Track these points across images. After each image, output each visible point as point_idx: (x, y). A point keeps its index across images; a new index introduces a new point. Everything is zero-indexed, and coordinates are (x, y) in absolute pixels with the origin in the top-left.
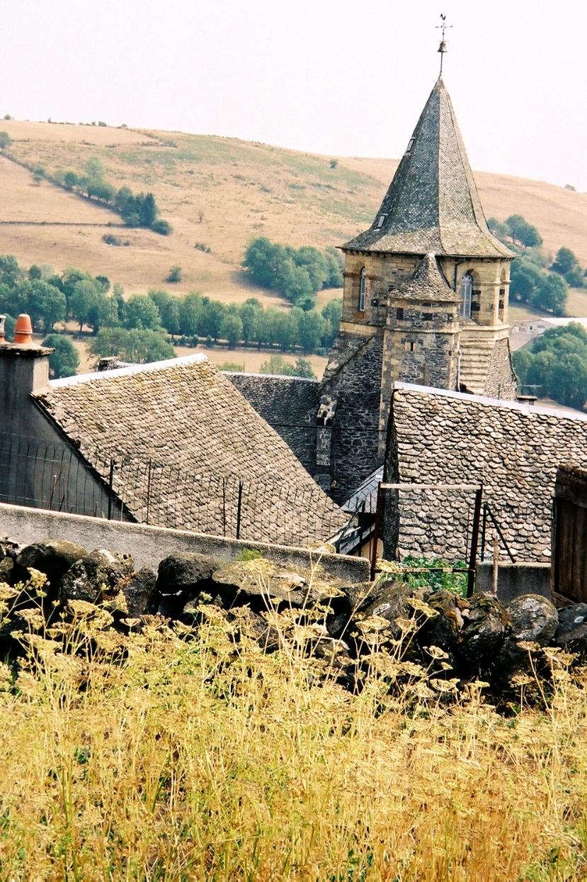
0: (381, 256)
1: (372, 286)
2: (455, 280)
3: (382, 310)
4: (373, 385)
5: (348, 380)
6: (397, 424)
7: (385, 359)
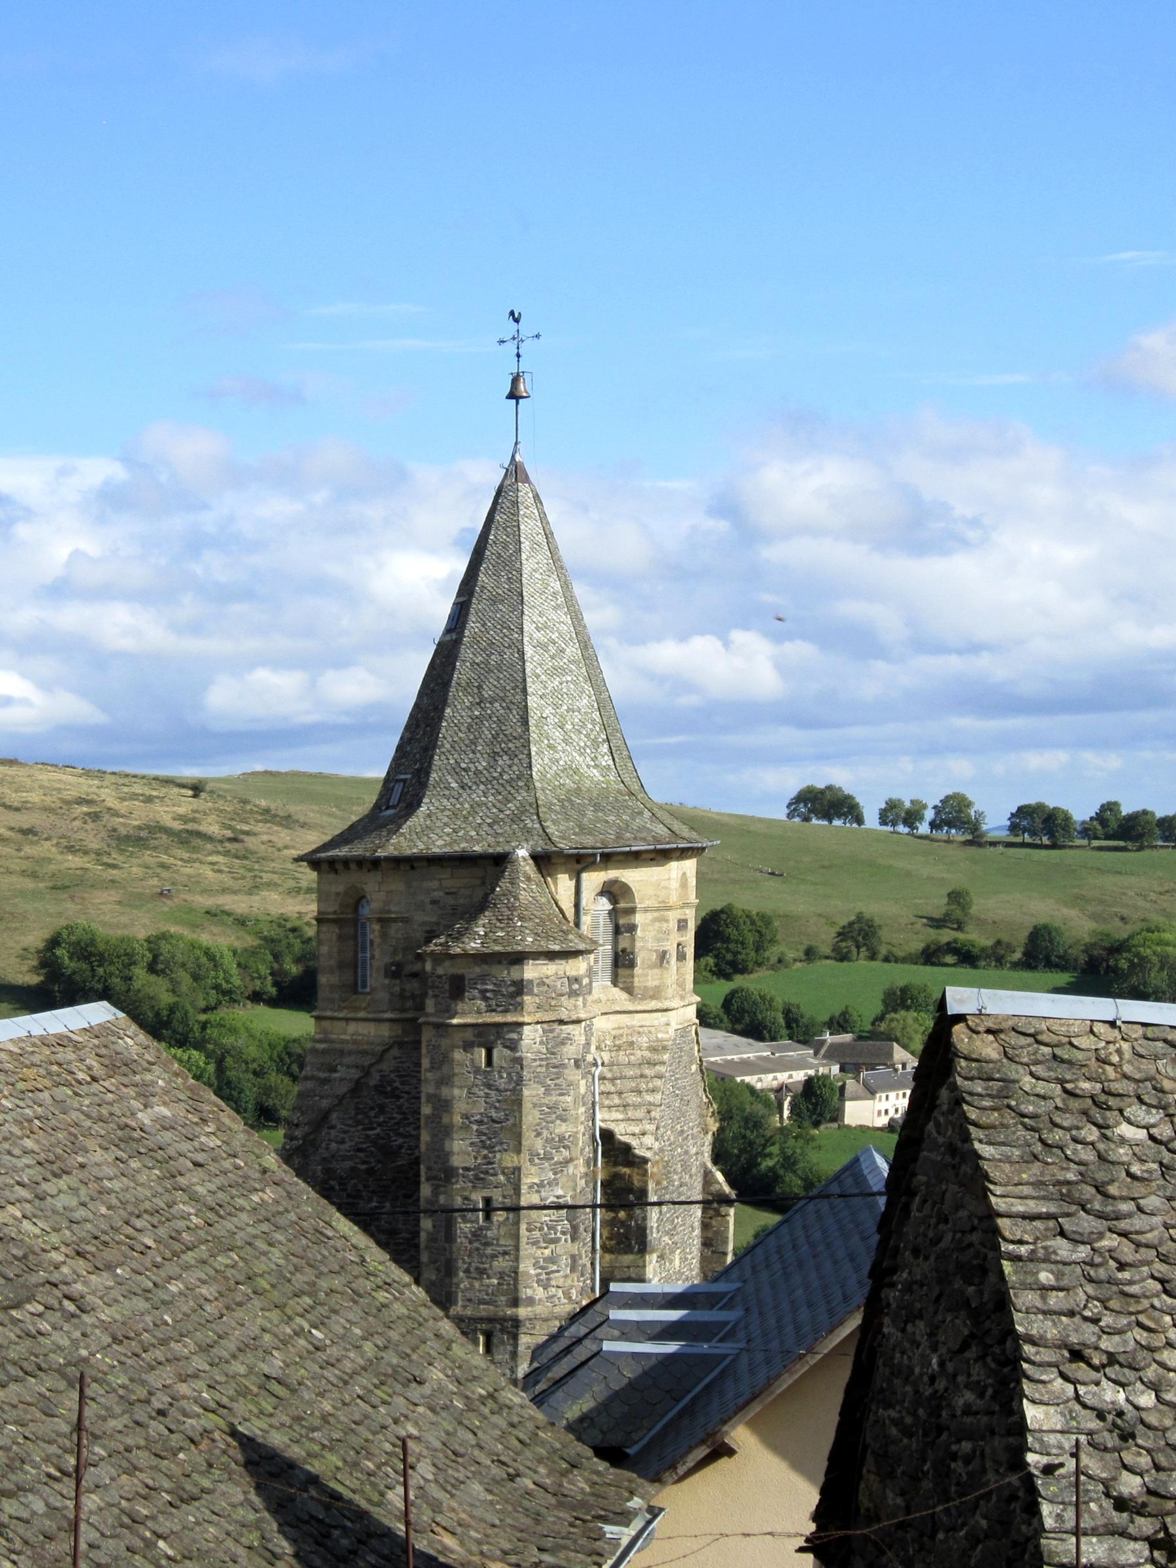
0: (403, 867)
1: (384, 935)
2: (577, 905)
3: (413, 986)
4: (400, 1147)
5: (342, 1142)
6: (985, 1150)
7: (427, 1089)
